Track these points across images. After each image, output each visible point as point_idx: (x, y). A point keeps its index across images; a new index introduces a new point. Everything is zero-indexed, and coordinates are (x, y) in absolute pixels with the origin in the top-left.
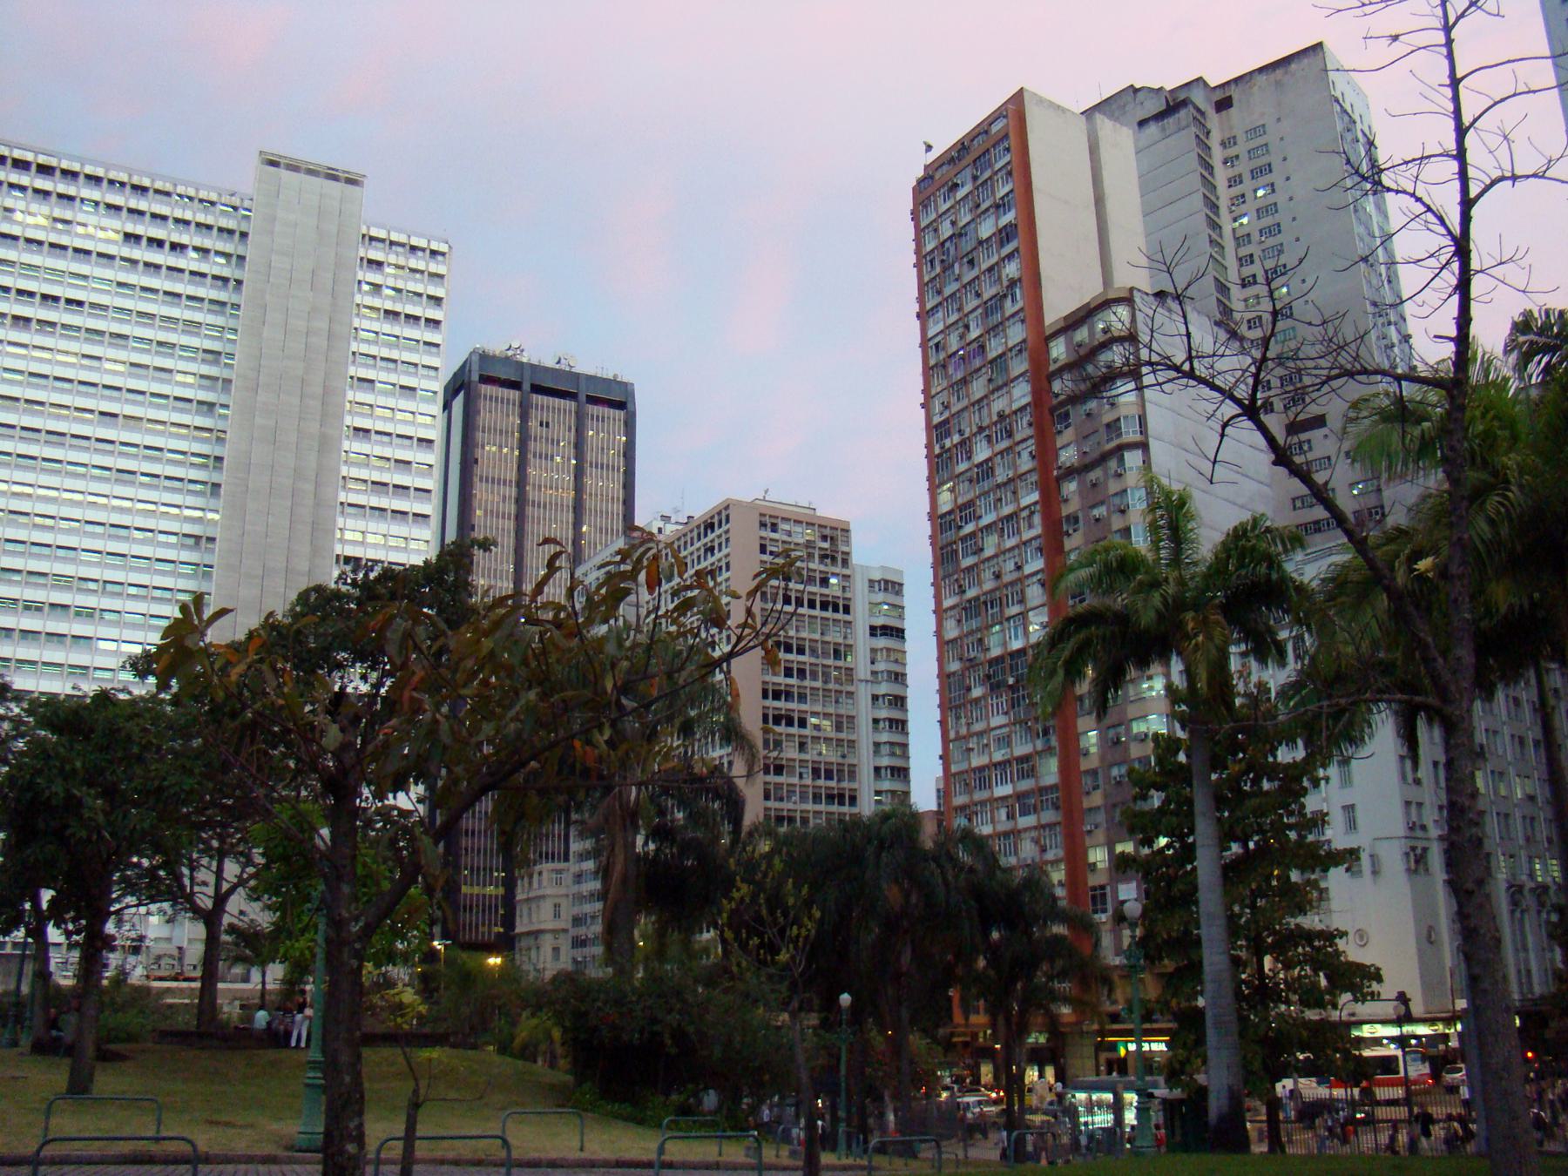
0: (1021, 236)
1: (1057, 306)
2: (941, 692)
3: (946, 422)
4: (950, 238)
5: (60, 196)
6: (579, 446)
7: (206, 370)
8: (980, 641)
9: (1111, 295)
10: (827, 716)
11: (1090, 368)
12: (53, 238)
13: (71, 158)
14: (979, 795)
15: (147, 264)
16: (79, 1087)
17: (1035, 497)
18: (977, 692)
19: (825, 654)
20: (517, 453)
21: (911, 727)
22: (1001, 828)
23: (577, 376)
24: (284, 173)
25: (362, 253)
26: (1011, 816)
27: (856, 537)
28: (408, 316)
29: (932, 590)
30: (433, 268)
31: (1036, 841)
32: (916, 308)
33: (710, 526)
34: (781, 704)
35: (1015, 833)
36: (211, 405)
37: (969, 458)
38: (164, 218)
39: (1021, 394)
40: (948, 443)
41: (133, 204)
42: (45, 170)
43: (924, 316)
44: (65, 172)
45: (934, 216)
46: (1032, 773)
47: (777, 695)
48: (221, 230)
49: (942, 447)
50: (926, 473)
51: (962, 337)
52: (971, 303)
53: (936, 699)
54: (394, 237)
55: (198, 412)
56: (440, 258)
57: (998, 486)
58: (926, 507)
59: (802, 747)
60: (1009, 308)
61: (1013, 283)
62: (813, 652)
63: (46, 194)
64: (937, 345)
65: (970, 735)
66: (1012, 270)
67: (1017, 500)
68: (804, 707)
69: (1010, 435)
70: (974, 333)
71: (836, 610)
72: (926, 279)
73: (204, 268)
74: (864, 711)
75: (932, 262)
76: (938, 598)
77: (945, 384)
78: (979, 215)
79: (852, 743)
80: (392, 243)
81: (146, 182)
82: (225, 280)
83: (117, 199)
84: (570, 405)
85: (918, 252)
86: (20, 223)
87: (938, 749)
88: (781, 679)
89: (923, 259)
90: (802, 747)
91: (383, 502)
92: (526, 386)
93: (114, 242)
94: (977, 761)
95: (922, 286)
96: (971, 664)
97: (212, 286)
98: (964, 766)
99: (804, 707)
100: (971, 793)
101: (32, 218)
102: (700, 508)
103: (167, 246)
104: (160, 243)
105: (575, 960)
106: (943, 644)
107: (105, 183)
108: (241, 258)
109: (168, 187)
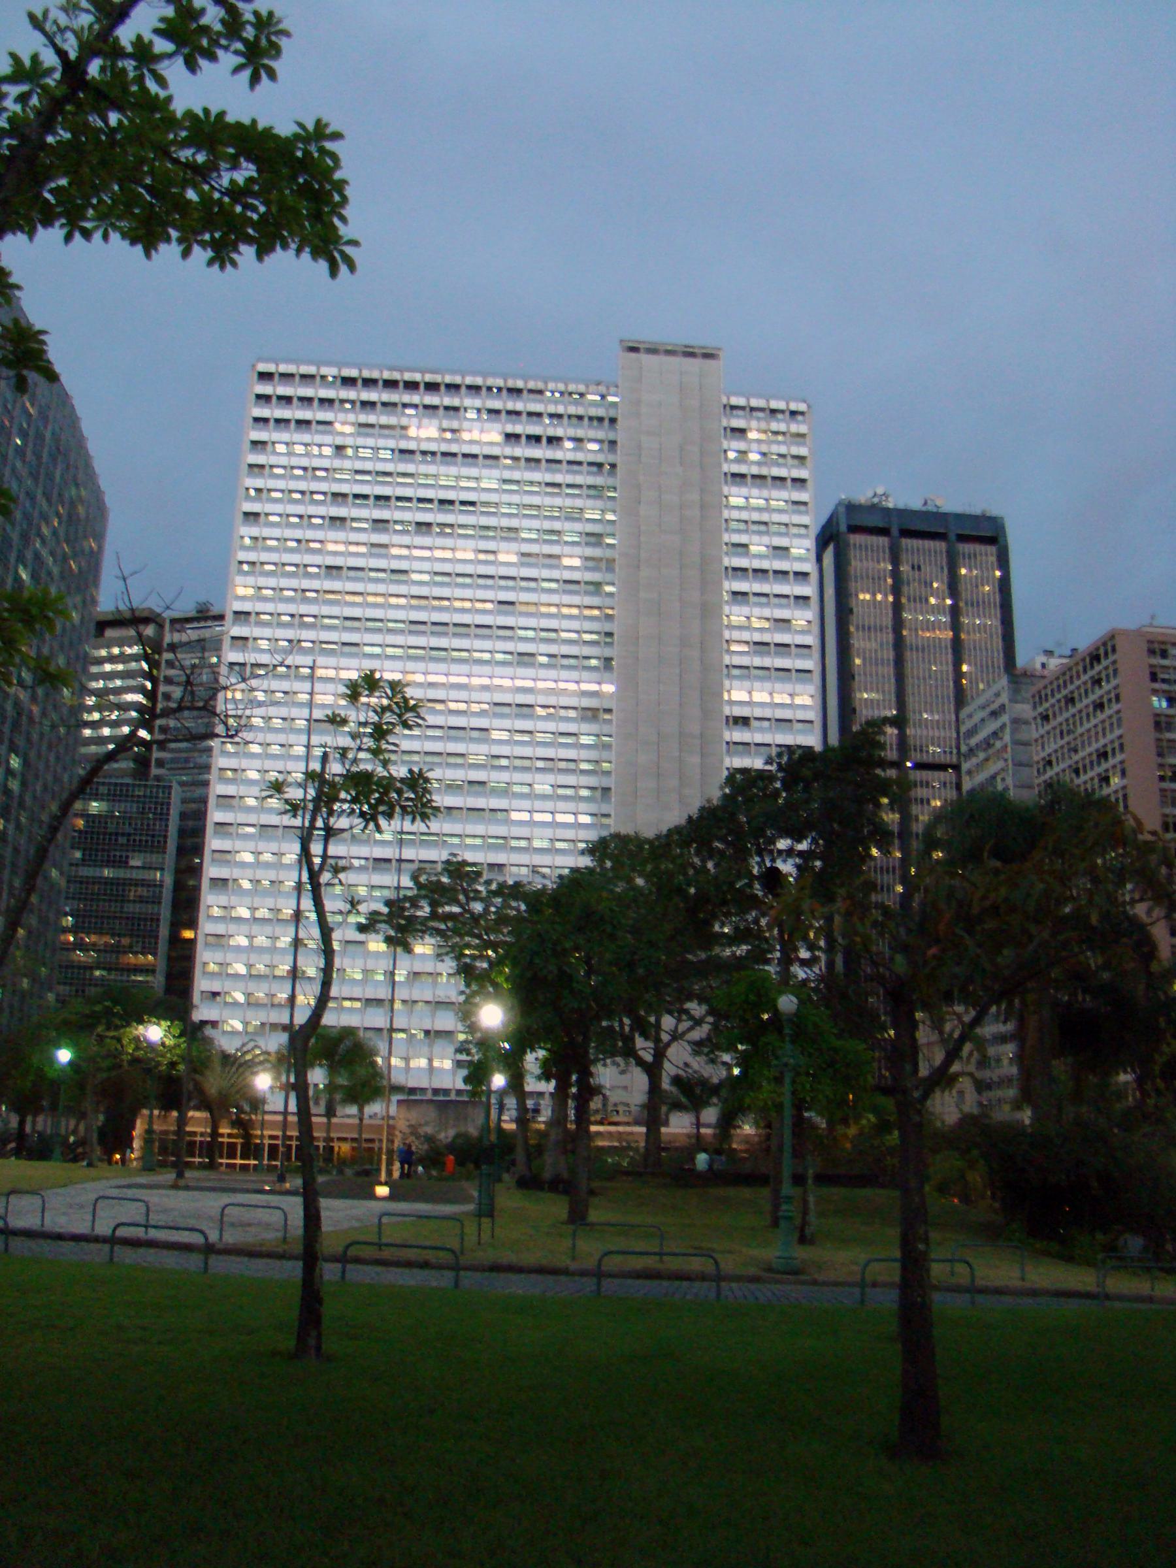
5: (447, 408)
7: (589, 552)
12: (444, 448)
13: (453, 372)
15: (528, 460)
16: (577, 1217)
20: (891, 599)
23: (945, 515)
24: (644, 357)
25: (725, 423)
28: (775, 478)
30: (794, 428)
33: (1095, 658)
36: (598, 585)
38: (539, 415)
41: (510, 406)
42: (432, 387)
48: (591, 419)
54: (754, 403)
55: (587, 593)
56: (800, 418)
63: (435, 407)
73: (580, 456)
80: (752, 409)
81: (520, 384)
82: (600, 465)
83: (496, 404)
84: (940, 546)
86: (412, 438)
91: (767, 662)
92: (895, 532)
97: (589, 473)
101: (426, 432)
102: (1085, 641)
103: (544, 440)
104: (537, 439)
105: (980, 1104)
107: (484, 390)
108: (613, 443)
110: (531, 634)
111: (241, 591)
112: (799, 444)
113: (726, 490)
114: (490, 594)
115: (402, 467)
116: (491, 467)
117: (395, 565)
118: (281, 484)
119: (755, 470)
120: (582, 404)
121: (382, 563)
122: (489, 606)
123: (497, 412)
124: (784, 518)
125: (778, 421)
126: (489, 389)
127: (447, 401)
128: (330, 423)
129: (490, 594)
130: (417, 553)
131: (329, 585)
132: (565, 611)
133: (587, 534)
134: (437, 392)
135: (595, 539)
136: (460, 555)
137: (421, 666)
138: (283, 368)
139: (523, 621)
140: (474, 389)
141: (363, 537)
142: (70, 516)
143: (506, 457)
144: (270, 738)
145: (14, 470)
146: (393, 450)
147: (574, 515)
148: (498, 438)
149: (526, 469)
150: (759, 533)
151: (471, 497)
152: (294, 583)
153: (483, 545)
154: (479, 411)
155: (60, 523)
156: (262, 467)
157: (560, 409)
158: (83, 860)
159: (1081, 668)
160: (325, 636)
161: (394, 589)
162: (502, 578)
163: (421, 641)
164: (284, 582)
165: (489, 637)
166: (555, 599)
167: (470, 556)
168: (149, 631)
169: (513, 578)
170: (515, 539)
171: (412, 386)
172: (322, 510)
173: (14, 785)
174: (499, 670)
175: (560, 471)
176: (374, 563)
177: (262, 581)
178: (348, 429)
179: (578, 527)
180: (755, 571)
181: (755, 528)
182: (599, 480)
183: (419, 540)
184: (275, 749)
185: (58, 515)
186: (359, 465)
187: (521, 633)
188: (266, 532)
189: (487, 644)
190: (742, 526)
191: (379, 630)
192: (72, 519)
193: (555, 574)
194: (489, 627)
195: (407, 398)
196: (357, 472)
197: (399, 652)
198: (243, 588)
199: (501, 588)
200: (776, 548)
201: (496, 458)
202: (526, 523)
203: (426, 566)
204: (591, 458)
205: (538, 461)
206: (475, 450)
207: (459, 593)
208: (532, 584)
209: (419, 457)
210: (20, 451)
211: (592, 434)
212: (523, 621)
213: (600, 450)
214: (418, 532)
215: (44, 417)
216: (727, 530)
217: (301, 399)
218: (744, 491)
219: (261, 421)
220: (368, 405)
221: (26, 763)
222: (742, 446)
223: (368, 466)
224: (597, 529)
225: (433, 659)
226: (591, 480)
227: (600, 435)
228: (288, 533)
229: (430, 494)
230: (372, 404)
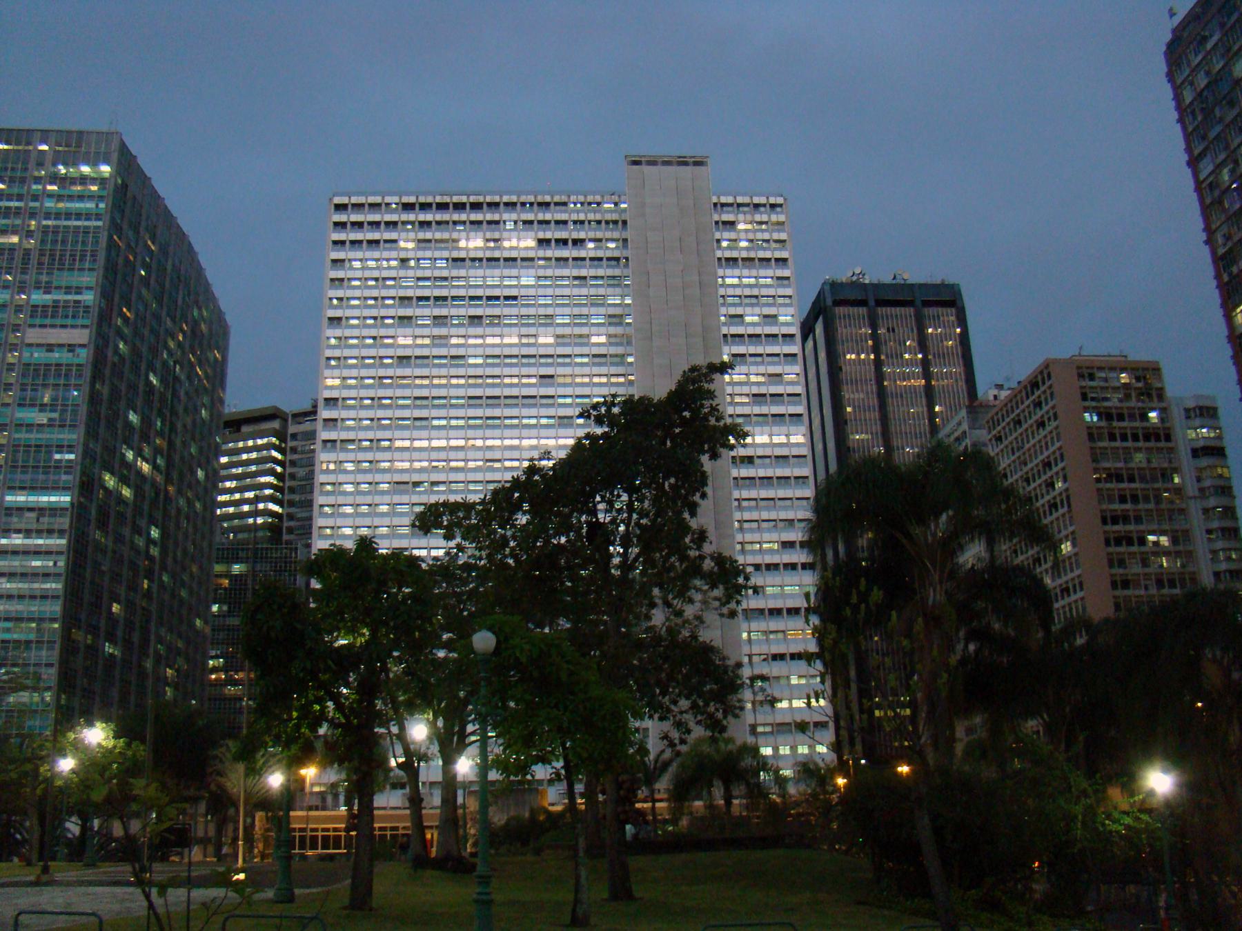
3: (1230, 251)
4: (1207, 86)
5: (489, 223)
6: (923, 344)
7: (612, 330)
10: (1163, 533)
12: (489, 254)
15: (558, 259)
19: (1154, 479)
20: (872, 357)
24: (646, 169)
25: (716, 217)
27: (1165, 372)
28: (761, 260)
30: (774, 218)
32: (1185, 157)
33: (1034, 385)
38: (565, 222)
41: (541, 217)
42: (476, 206)
43: (1193, 163)
44: (490, 205)
45: (1187, 72)
47: (1115, 520)
48: (607, 222)
49: (1230, 274)
51: (1232, 172)
54: (740, 200)
55: (613, 364)
56: (779, 209)
58: (1224, 331)
59: (1145, 563)
62: (1143, 479)
63: (480, 223)
64: (1211, 184)
68: (1142, 527)
71: (1158, 439)
72: (1190, 129)
73: (600, 254)
74: (1196, 522)
75: (1193, 113)
77: (1223, 218)
79: (1189, 555)
80: (739, 205)
81: (548, 199)
82: (617, 259)
83: (530, 217)
85: (1179, 108)
86: (462, 249)
88: (1116, 506)
90: (1145, 563)
91: (764, 410)
93: (531, 248)
95: (1188, 137)
97: (608, 266)
99: (1142, 527)
101: (474, 243)
102: (1024, 372)
103: (570, 242)
104: (564, 242)
108: (625, 240)
109: (564, 199)
110: (569, 401)
111: (329, 382)
112: (779, 231)
113: (720, 272)
114: (533, 371)
115: (455, 273)
116: (527, 267)
117: (454, 352)
118: (357, 293)
119: (744, 254)
120: (599, 211)
121: (443, 351)
122: (533, 381)
123: (531, 222)
124: (771, 292)
125: (761, 213)
126: (523, 204)
127: (489, 217)
128: (395, 241)
129: (533, 371)
130: (471, 341)
131: (400, 372)
132: (596, 380)
133: (610, 316)
134: (480, 210)
135: (615, 319)
136: (507, 340)
137: (479, 433)
138: (354, 200)
139: (561, 391)
140: (511, 205)
141: (426, 331)
142: (193, 332)
143: (539, 259)
144: (359, 499)
145: (140, 297)
146: (447, 259)
148: (531, 243)
149: (557, 267)
150: (752, 305)
151: (514, 292)
152: (372, 372)
153: (524, 331)
154: (515, 222)
155: (184, 337)
156: (342, 280)
157: (582, 217)
158: (229, 611)
159: (1024, 394)
160: (399, 413)
161: (453, 372)
162: (541, 356)
164: (364, 372)
165: (534, 405)
166: (586, 370)
167: (515, 340)
168: (276, 424)
169: (551, 356)
170: (551, 325)
171: (459, 207)
172: (391, 312)
173: (155, 551)
174: (544, 432)
175: (584, 267)
176: (436, 352)
177: (346, 373)
178: (411, 245)
179: (602, 310)
180: (750, 336)
181: (747, 301)
184: (364, 509)
185: (182, 330)
186: (420, 274)
187: (561, 401)
188: (348, 333)
189: (533, 412)
190: (737, 300)
191: (444, 406)
192: (195, 332)
193: (585, 350)
194: (534, 397)
196: (419, 279)
197: (461, 422)
199: (542, 365)
200: (765, 316)
201: (532, 259)
202: (559, 311)
203: (480, 351)
204: (609, 254)
205: (566, 259)
206: (514, 254)
207: (507, 371)
208: (568, 360)
209: (468, 263)
210: (145, 281)
213: (617, 248)
214: (471, 324)
215: (164, 250)
216: (723, 305)
217: (370, 223)
218: (737, 272)
220: (425, 225)
221: (164, 534)
222: (733, 235)
223: (428, 273)
224: (618, 311)
225: (488, 427)
226: (610, 272)
227: (616, 235)
228: (366, 332)
229: (479, 292)
230: (429, 224)
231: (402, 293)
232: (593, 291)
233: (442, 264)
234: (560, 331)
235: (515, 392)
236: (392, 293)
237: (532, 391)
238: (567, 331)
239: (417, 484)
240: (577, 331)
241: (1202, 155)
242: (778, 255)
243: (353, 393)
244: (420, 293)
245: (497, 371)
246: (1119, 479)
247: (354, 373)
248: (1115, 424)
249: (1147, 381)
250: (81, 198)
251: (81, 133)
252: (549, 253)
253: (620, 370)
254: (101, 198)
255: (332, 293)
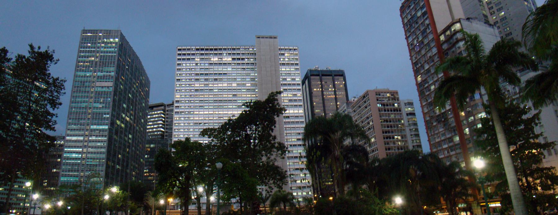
0: (428, 13)
1: (440, 27)
2: (426, 125)
3: (416, 62)
7: (252, 82)
8: (434, 111)
9: (454, 21)
10: (399, 135)
11: (451, 41)
14: (439, 148)
17: (442, 74)
18: (435, 124)
19: (396, 121)
21: (420, 135)
22: (446, 155)
24: (261, 39)
26: (448, 152)
27: (399, 93)
29: (419, 102)
31: (456, 157)
33: (364, 97)
34: (388, 134)
35: (451, 156)
37: (424, 69)
39: (435, 50)
40: (418, 66)
41: (233, 52)
42: (216, 49)
43: (407, 38)
44: (219, 49)
46: (452, 141)
47: (386, 132)
50: (413, 75)
51: (417, 41)
52: (418, 32)
53: (425, 127)
54: (286, 48)
57: (432, 74)
58: (415, 83)
59: (394, 143)
60: (428, 31)
61: (428, 25)
62: (393, 122)
65: (434, 135)
66: (427, 22)
67: (437, 76)
68: (393, 134)
69: (433, 61)
70: (420, 39)
71: (397, 111)
73: (249, 62)
76: (421, 103)
78: (416, 11)
79: (406, 141)
83: (230, 52)
87: (427, 139)
88: (386, 129)
89: (404, 25)
90: (394, 143)
91: (292, 104)
94: (437, 140)
95: (405, 31)
96: (432, 117)
98: (434, 142)
99: (393, 134)
100: (437, 148)
101: (215, 59)
102: (361, 93)
104: (239, 59)
106: (424, 114)
111: (177, 96)
114: (231, 93)
115: (210, 67)
117: (210, 88)
118: (184, 73)
121: (207, 88)
127: (219, 52)
131: (196, 94)
134: (217, 51)
135: (253, 80)
136: (224, 85)
137: (217, 110)
139: (238, 99)
141: (203, 83)
145: (126, 73)
147: (248, 75)
148: (231, 59)
151: (226, 72)
152: (188, 94)
153: (229, 83)
160: (196, 105)
161: (210, 93)
163: (217, 104)
164: (186, 94)
166: (245, 93)
167: (226, 85)
168: (163, 108)
171: (211, 50)
172: (193, 78)
176: (205, 88)
177: (181, 94)
179: (249, 77)
182: (253, 67)
183: (215, 83)
184: (186, 130)
186: (201, 67)
188: (182, 83)
189: (231, 104)
192: (141, 83)
193: (245, 88)
195: (210, 52)
198: (177, 96)
202: (238, 77)
206: (226, 62)
211: (251, 57)
212: (238, 99)
215: (133, 61)
219: (179, 59)
220: (202, 54)
221: (133, 137)
222: (284, 57)
223: (203, 67)
224: (253, 77)
226: (251, 67)
227: (253, 57)
228: (187, 83)
229: (217, 72)
231: (196, 73)
232: (247, 72)
233: (207, 65)
234: (238, 83)
235: (226, 99)
236: (194, 72)
237: (231, 99)
238: (240, 83)
239: (200, 123)
240: (243, 83)
241: (409, 36)
242: (296, 62)
243: (183, 99)
244: (201, 72)
245: (221, 93)
246: (387, 121)
247: (184, 94)
248: (386, 107)
249: (394, 96)
250: (110, 47)
251: (110, 30)
252: (235, 62)
253: (254, 93)
254: (116, 47)
255: (177, 73)
